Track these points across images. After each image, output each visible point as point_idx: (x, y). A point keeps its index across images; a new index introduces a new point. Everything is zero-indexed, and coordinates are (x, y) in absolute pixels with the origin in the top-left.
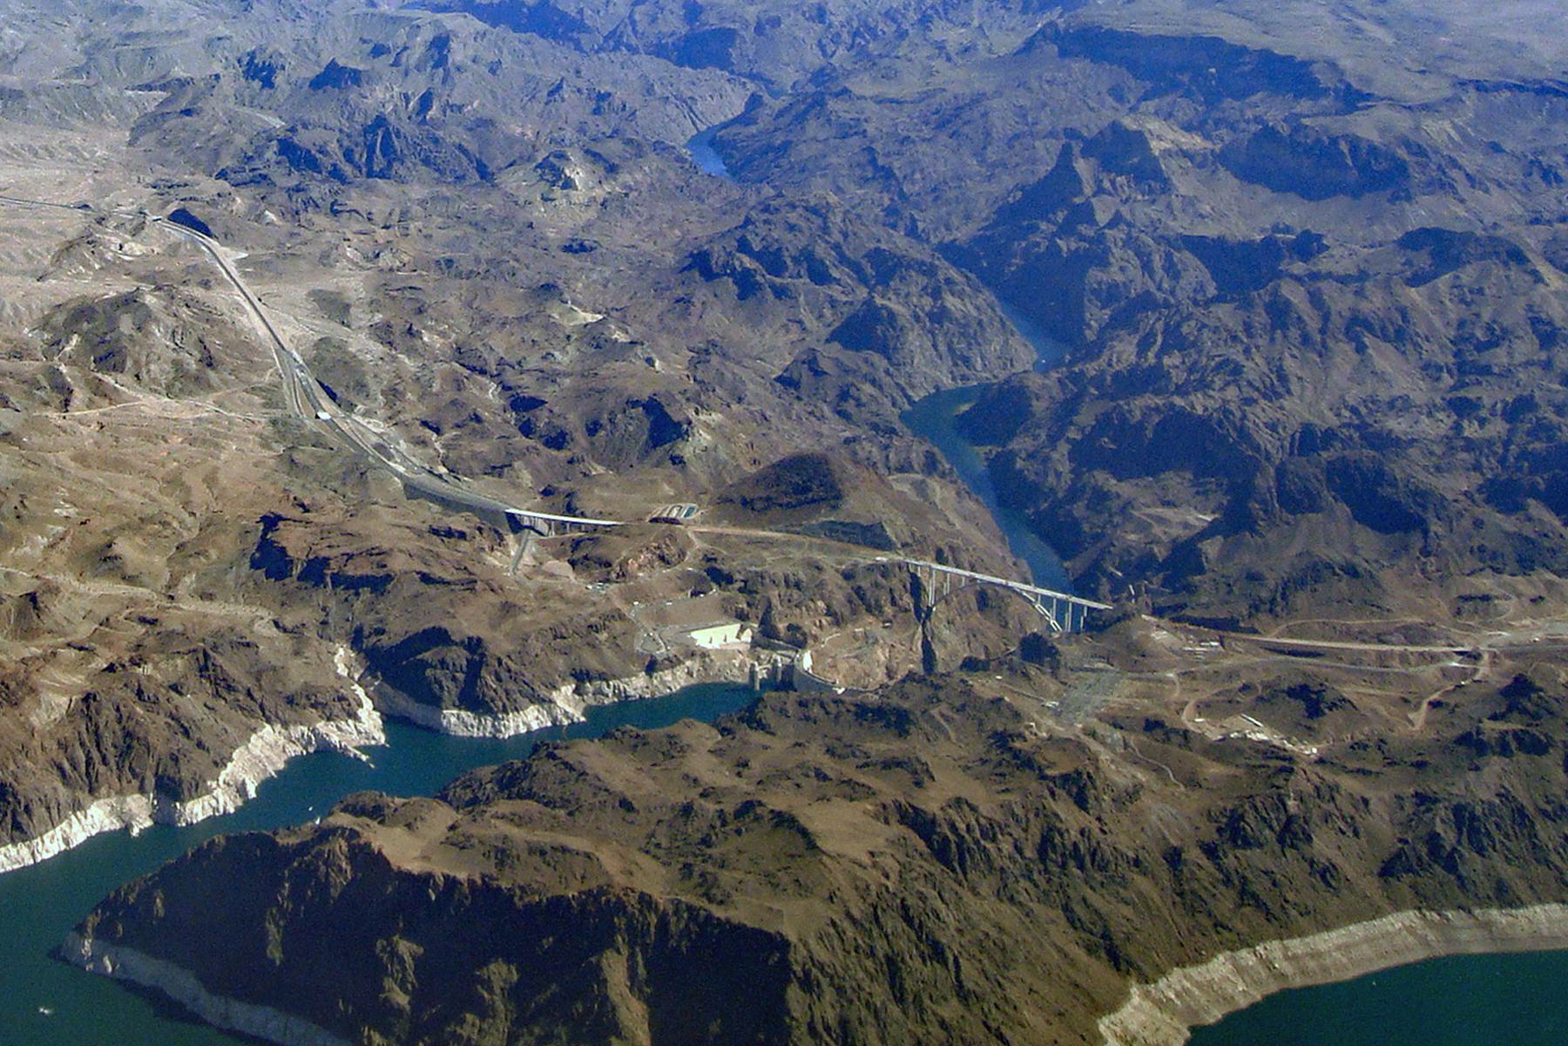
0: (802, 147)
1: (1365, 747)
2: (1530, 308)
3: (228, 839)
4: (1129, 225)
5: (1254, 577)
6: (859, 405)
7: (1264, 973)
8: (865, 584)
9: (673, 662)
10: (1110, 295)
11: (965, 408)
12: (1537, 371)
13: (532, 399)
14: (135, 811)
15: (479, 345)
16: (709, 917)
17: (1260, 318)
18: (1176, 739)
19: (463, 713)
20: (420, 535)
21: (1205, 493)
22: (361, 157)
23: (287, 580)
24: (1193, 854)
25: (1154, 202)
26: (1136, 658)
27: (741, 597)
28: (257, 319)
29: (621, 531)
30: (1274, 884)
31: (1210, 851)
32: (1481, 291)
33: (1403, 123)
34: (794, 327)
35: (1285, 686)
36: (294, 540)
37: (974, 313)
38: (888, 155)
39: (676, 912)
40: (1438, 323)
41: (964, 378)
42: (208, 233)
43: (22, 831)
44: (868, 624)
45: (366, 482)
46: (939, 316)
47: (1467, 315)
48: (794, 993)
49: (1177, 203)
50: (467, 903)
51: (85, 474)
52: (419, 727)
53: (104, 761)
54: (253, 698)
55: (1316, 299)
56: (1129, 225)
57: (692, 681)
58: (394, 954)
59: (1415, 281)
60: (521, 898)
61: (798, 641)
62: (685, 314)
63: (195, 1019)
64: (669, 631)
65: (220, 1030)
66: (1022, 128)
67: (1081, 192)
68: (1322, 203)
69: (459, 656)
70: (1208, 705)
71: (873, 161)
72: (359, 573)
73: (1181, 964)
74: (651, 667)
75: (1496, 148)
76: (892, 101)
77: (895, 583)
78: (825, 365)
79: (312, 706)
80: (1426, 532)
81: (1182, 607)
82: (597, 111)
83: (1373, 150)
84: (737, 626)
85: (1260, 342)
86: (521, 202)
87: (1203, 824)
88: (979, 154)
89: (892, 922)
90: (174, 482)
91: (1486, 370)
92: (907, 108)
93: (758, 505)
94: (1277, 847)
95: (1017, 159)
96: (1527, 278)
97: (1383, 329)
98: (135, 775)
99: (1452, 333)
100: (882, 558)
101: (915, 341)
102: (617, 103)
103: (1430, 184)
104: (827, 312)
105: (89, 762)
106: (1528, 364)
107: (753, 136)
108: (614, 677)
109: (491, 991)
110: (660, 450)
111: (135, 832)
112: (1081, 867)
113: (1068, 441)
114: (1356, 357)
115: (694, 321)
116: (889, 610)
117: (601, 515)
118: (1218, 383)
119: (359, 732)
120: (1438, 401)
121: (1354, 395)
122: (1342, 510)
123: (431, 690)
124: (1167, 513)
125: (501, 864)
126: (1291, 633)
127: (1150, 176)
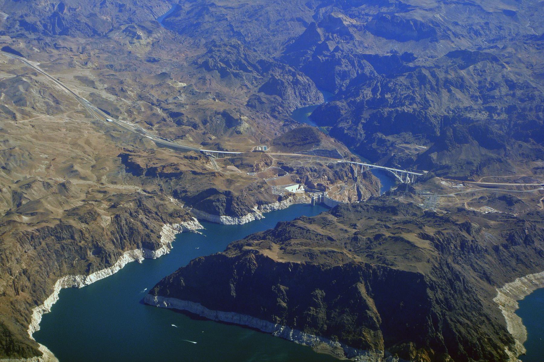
0: (205, 24)
1: (533, 214)
2: (503, 76)
3: (205, 257)
4: (342, 51)
5: (469, 163)
6: (279, 113)
7: (531, 284)
8: (338, 170)
9: (286, 197)
10: (344, 75)
11: (310, 114)
12: (510, 97)
13: (177, 113)
14: (138, 255)
15: (148, 95)
16: (391, 270)
17: (416, 81)
18: (472, 214)
19: (227, 217)
20: (181, 158)
21: (419, 139)
22: (50, 27)
23: (142, 176)
24: (501, 248)
25: (348, 43)
26: (440, 190)
27: (297, 175)
28: (62, 87)
29: (246, 155)
30: (526, 256)
31: (505, 247)
32: (484, 71)
33: (430, 15)
34: (244, 87)
35: (497, 196)
36: (141, 162)
37: (307, 81)
38: (238, 27)
39: (379, 269)
40: (472, 82)
41: (305, 104)
42: (22, 56)
43: (109, 263)
44: (340, 183)
45: (143, 143)
46: (296, 83)
47: (481, 79)
48: (428, 291)
49: (356, 43)
50: (302, 271)
51: (40, 142)
52: (212, 222)
53: (125, 237)
54: (158, 215)
55: (433, 75)
56: (342, 51)
57: (292, 204)
58: (279, 290)
59: (462, 68)
60: (323, 268)
61: (322, 189)
62: (204, 83)
63: (204, 319)
64: (278, 187)
65: (215, 321)
66: (280, 18)
67: (320, 40)
68: (405, 43)
69: (223, 198)
70: (471, 204)
71: (232, 30)
72: (169, 172)
73: (507, 282)
74: (280, 199)
75: (456, 24)
76: (230, 8)
77: (346, 169)
78: (264, 100)
79: (179, 217)
80: (505, 149)
81: (448, 173)
82: (120, 11)
83: (422, 24)
84: (297, 186)
85: (417, 89)
86: (122, 44)
87: (500, 238)
88: (267, 26)
89: (446, 269)
90: (74, 144)
91: (493, 97)
92: (236, 10)
93: (290, 145)
94: (524, 245)
95: (281, 29)
96: (500, 67)
97: (456, 84)
98: (135, 243)
99: (477, 85)
100: (340, 161)
101: (290, 91)
102: (128, 8)
103: (443, 36)
104: (255, 82)
105: (121, 239)
106: (507, 95)
107: (180, 20)
108: (270, 203)
109: (317, 299)
110: (231, 130)
111: (141, 262)
112: (473, 252)
113: (362, 123)
114: (448, 94)
115: (208, 86)
116: (346, 178)
117: (233, 150)
118: (407, 103)
119: (195, 225)
120: (482, 108)
121: (452, 107)
122: (475, 142)
123: (215, 209)
124: (408, 146)
125: (311, 258)
126: (484, 180)
127: (345, 34)
